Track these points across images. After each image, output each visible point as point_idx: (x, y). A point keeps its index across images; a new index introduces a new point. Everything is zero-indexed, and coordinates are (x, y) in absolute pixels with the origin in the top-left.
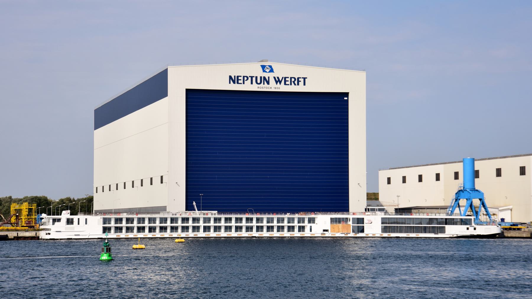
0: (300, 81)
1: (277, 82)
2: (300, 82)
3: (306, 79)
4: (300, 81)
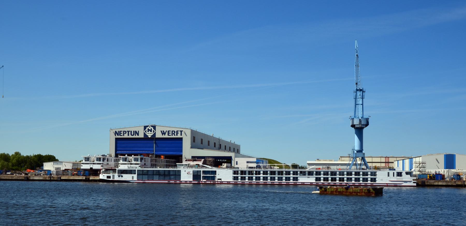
0: (178, 133)
4: (178, 133)
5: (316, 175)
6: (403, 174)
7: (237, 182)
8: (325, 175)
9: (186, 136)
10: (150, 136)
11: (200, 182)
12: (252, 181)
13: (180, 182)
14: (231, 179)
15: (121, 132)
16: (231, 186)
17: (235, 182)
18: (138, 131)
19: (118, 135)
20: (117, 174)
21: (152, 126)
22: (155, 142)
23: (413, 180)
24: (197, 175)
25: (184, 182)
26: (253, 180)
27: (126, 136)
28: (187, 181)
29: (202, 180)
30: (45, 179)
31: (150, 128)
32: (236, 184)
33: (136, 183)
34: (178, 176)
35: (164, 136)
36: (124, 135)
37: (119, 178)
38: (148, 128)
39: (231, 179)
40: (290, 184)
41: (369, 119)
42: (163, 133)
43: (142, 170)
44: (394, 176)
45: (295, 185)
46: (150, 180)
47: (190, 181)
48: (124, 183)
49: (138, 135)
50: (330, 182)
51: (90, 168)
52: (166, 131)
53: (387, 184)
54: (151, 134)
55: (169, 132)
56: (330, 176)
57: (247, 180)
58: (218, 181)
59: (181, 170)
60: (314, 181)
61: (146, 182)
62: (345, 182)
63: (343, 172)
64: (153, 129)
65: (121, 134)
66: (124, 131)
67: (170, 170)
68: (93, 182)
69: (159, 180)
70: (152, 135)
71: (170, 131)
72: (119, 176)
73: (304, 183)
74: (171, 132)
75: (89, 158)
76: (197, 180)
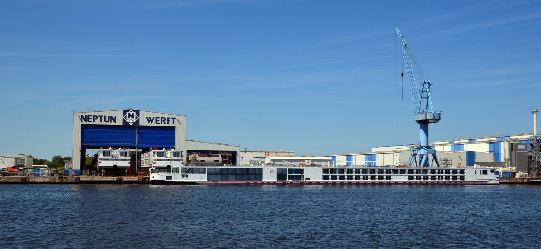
0: (170, 121)
1: (149, 122)
2: (169, 122)
3: (175, 119)
4: (170, 121)
5: (409, 173)
6: (488, 172)
7: (327, 182)
8: (432, 174)
9: (180, 124)
10: (131, 124)
11: (285, 182)
12: (344, 181)
13: (261, 182)
14: (321, 179)
15: (90, 117)
16: (320, 187)
17: (325, 182)
18: (115, 117)
19: (85, 121)
20: (181, 174)
21: (134, 111)
22: (138, 131)
23: (497, 178)
24: (281, 173)
25: (267, 183)
26: (328, 180)
27: (97, 122)
28: (269, 182)
29: (287, 180)
30: (54, 181)
31: (131, 114)
32: (326, 184)
33: (206, 185)
34: (259, 175)
35: (150, 124)
36: (94, 121)
37: (183, 178)
38: (129, 112)
39: (321, 179)
40: (360, 183)
41: (440, 114)
42: (149, 119)
43: (214, 168)
44: (480, 174)
45: (389, 184)
46: (224, 181)
47: (273, 182)
48: (188, 185)
49: (115, 121)
50: (422, 180)
51: (113, 165)
52: (154, 118)
53: (474, 182)
54: (133, 120)
55: (158, 119)
56: (423, 174)
57: (338, 180)
58: (306, 181)
59: (262, 168)
60: (407, 180)
61: (219, 183)
62: (437, 180)
63: (383, 170)
64: (135, 115)
65: (90, 120)
66: (94, 116)
67: (249, 168)
68: (114, 184)
69: (236, 180)
70: (134, 122)
71: (159, 118)
72: (183, 176)
73: (397, 182)
74: (160, 119)
75: (109, 152)
76: (282, 180)
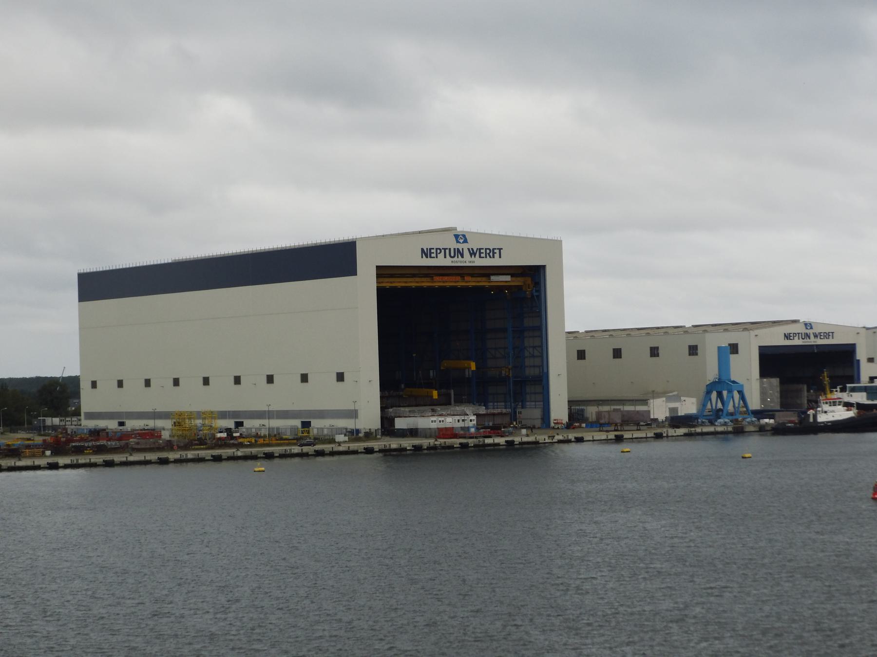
0: (496, 253)
4: (496, 253)
